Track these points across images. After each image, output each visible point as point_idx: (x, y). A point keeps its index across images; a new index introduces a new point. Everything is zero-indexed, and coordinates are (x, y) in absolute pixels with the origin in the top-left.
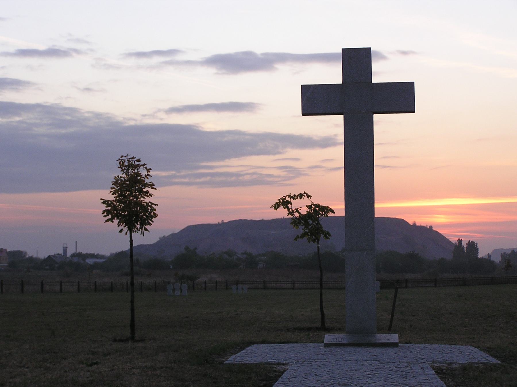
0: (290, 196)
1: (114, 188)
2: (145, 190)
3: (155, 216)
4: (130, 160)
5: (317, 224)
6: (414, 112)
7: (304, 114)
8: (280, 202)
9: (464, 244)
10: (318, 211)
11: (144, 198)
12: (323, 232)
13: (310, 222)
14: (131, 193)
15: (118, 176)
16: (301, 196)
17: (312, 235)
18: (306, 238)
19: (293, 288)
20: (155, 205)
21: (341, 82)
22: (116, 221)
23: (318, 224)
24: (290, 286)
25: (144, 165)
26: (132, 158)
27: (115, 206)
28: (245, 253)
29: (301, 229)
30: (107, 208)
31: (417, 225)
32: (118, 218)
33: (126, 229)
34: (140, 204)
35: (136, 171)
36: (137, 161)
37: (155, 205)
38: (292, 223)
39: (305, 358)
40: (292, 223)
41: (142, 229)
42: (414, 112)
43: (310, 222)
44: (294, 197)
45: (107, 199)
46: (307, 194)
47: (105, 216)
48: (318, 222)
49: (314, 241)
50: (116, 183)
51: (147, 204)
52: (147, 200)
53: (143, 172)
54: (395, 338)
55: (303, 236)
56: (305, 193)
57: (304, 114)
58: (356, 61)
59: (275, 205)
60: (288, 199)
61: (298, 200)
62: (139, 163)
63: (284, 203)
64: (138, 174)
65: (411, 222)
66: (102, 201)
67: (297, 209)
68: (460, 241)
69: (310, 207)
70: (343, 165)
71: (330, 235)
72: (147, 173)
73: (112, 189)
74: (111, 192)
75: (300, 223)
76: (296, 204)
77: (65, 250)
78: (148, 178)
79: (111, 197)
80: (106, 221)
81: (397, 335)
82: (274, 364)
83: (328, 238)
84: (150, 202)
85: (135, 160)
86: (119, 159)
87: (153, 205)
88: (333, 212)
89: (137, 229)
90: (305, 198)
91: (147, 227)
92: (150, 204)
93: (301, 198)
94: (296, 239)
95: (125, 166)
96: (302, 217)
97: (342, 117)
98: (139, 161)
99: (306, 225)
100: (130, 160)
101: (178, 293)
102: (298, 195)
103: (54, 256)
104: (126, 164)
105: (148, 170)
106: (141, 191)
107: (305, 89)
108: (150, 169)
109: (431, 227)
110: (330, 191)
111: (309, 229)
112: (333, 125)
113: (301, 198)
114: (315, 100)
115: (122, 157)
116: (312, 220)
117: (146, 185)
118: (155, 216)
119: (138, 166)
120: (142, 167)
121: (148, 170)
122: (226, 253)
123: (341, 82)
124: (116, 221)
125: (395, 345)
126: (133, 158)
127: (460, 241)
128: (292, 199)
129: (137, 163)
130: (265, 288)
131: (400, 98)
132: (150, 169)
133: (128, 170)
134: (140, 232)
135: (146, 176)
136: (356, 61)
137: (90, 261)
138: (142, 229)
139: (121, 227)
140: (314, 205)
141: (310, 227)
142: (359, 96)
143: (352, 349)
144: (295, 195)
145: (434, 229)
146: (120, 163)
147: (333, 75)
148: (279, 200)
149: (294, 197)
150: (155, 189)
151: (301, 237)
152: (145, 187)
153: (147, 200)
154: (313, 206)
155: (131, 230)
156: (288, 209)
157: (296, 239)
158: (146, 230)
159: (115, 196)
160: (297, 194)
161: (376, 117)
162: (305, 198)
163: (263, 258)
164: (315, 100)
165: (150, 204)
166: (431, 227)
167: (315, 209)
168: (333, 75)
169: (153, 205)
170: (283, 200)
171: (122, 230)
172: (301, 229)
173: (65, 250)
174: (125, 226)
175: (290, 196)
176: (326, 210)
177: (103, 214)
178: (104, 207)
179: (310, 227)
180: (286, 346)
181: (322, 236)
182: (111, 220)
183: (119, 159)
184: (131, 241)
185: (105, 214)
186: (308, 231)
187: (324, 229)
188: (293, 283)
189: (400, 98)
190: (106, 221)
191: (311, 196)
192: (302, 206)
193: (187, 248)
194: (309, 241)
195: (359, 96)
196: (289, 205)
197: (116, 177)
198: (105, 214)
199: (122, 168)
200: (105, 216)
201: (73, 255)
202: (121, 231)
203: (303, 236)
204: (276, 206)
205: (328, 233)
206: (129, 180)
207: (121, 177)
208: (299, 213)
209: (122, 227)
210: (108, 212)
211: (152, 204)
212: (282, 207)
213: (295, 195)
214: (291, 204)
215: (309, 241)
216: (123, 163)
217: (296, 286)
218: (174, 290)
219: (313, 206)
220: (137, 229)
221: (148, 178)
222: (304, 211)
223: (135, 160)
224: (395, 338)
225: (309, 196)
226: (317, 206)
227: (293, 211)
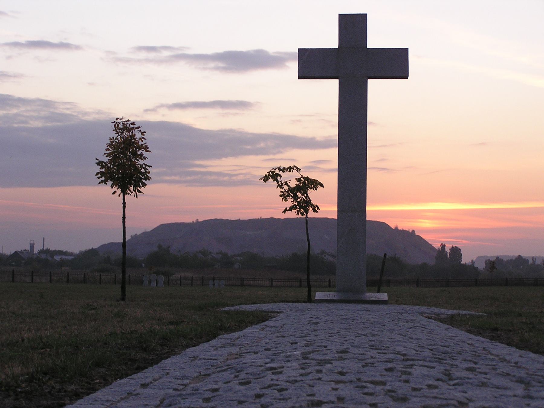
0: (279, 169)
1: (109, 150)
2: (139, 153)
3: (148, 178)
4: (125, 123)
5: (306, 197)
6: (407, 77)
7: (300, 78)
8: (269, 175)
9: (448, 249)
11: (138, 160)
12: (312, 205)
13: (299, 195)
14: (125, 156)
15: (113, 138)
16: (290, 169)
18: (294, 211)
19: (271, 286)
20: (149, 166)
21: (337, 47)
22: (110, 183)
24: (268, 283)
26: (126, 121)
27: (108, 167)
28: (221, 253)
29: (290, 202)
30: (101, 170)
31: (399, 229)
32: (111, 180)
33: (119, 191)
34: (134, 165)
37: (149, 166)
38: (280, 196)
39: (298, 307)
40: (280, 196)
41: (135, 191)
42: (407, 77)
43: (299, 195)
44: (283, 170)
45: (101, 160)
47: (99, 178)
48: (307, 195)
49: (303, 214)
50: (110, 145)
51: (141, 166)
52: (141, 162)
53: (138, 135)
54: (384, 296)
55: (291, 209)
56: (294, 166)
57: (300, 78)
58: (353, 26)
59: (264, 177)
60: (277, 171)
61: (288, 173)
63: (273, 176)
64: (133, 136)
65: (393, 226)
66: (98, 161)
68: (443, 246)
69: (299, 180)
70: (334, 132)
71: (318, 209)
72: (141, 136)
73: (106, 150)
74: (105, 154)
75: (289, 196)
76: (285, 176)
77: (32, 246)
78: (142, 141)
79: (106, 159)
80: (100, 183)
81: (386, 294)
82: (269, 312)
83: (316, 211)
84: (144, 164)
85: (129, 123)
86: (115, 122)
87: (147, 167)
88: (322, 185)
89: (130, 191)
91: (142, 189)
92: (144, 166)
93: (290, 171)
94: (284, 212)
95: (120, 129)
96: (291, 190)
97: (337, 81)
98: (133, 124)
99: (295, 197)
100: (125, 123)
101: (154, 284)
103: (21, 252)
104: (121, 126)
105: (143, 133)
106: (135, 154)
108: (145, 132)
109: (413, 231)
111: (298, 202)
112: (328, 91)
114: (312, 64)
115: (117, 119)
116: (301, 193)
117: (140, 147)
118: (148, 178)
119: (133, 128)
120: (137, 130)
121: (143, 133)
122: (200, 252)
123: (337, 47)
124: (110, 183)
125: (384, 302)
126: (128, 121)
127: (443, 246)
128: (281, 172)
129: (131, 126)
130: (242, 285)
131: (394, 64)
132: (145, 132)
133: (123, 132)
134: (133, 194)
135: (140, 139)
136: (353, 26)
137: (57, 258)
138: (135, 191)
139: (115, 189)
141: (299, 200)
142: (354, 62)
143: (343, 305)
144: (284, 168)
145: (417, 234)
147: (329, 39)
148: (269, 172)
150: (150, 151)
151: (289, 210)
152: (140, 149)
153: (141, 162)
154: (302, 179)
155: (124, 192)
156: (278, 182)
157: (284, 212)
158: (139, 192)
159: (108, 158)
160: (287, 167)
164: (312, 64)
165: (144, 166)
166: (413, 231)
167: (304, 182)
168: (329, 39)
169: (147, 167)
170: (273, 172)
171: (115, 191)
172: (290, 202)
173: (32, 246)
174: (119, 188)
176: (315, 184)
177: (97, 175)
178: (98, 169)
179: (299, 200)
181: (311, 209)
182: (105, 182)
184: (124, 203)
185: (99, 175)
186: (296, 204)
187: (312, 202)
188: (271, 280)
189: (394, 64)
190: (100, 183)
191: (300, 170)
193: (160, 247)
194: (298, 214)
195: (354, 62)
197: (111, 139)
198: (99, 175)
199: (116, 131)
200: (99, 178)
201: (42, 252)
202: (114, 193)
203: (291, 209)
204: (265, 179)
205: (317, 206)
206: (124, 142)
207: (116, 139)
208: (289, 186)
210: (102, 174)
211: (146, 165)
214: (281, 176)
215: (298, 214)
216: (118, 125)
217: (274, 283)
218: (150, 282)
219: (302, 179)
220: (130, 191)
221: (142, 141)
222: (293, 184)
223: (129, 123)
224: (384, 296)
225: (298, 170)
226: (307, 179)
227: (282, 184)
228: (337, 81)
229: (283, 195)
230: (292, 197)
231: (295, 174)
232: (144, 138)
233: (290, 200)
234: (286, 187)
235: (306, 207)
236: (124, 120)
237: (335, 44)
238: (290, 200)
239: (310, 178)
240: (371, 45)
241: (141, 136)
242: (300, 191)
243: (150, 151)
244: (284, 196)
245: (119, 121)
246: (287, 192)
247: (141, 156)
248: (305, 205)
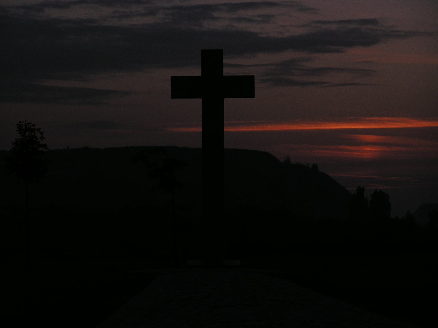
25: (39, 129)
26: (29, 124)
35: (33, 134)
53: (38, 135)
58: (212, 59)
62: (35, 127)
72: (41, 136)
78: (42, 140)
85: (30, 125)
98: (34, 125)
105: (42, 133)
108: (43, 132)
114: (181, 88)
115: (20, 122)
121: (42, 133)
123: (200, 75)
126: (30, 123)
129: (32, 127)
131: (244, 87)
135: (41, 138)
146: (18, 127)
161: (226, 100)
164: (181, 88)
183: (18, 124)
189: (244, 87)
195: (214, 84)
221: (42, 140)
232: (43, 138)
241: (41, 136)
243: (48, 149)
245: (22, 123)
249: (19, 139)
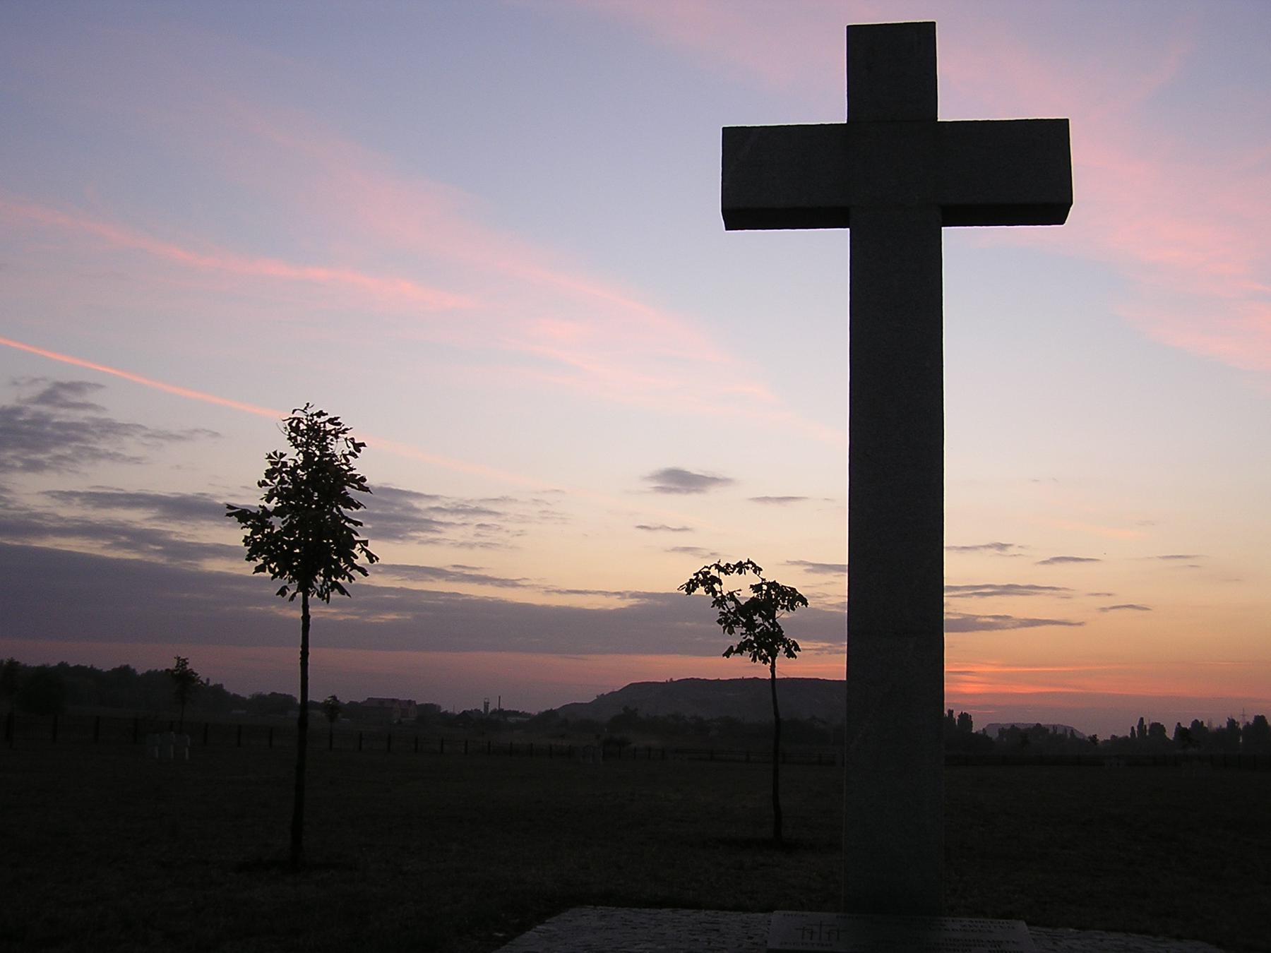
10: (775, 597)
12: (785, 641)
15: (275, 453)
16: (741, 567)
17: (760, 648)
18: (746, 652)
23: (775, 625)
36: (331, 421)
37: (357, 523)
38: (720, 622)
40: (720, 622)
43: (758, 619)
44: (726, 570)
46: (754, 565)
49: (766, 661)
53: (339, 447)
55: (741, 649)
56: (749, 562)
58: (891, 61)
59: (688, 584)
60: (714, 572)
63: (706, 580)
67: (731, 594)
69: (756, 588)
71: (797, 649)
75: (737, 622)
85: (323, 419)
88: (804, 602)
90: (750, 572)
93: (740, 572)
94: (727, 654)
97: (842, 236)
99: (750, 626)
102: (735, 566)
107: (733, 138)
108: (363, 445)
110: (803, 535)
113: (740, 572)
114: (767, 180)
126: (320, 414)
129: (329, 427)
132: (363, 445)
136: (891, 61)
140: (768, 584)
144: (728, 565)
146: (290, 424)
148: (696, 574)
149: (726, 570)
154: (765, 587)
155: (305, 587)
158: (343, 591)
160: (733, 562)
162: (750, 572)
163: (377, 512)
167: (768, 591)
172: (737, 637)
175: (717, 566)
176: (793, 598)
180: (666, 913)
191: (760, 569)
192: (740, 586)
194: (754, 660)
196: (716, 586)
197: (270, 457)
202: (282, 592)
204: (691, 586)
208: (737, 602)
209: (286, 582)
212: (701, 590)
213: (728, 565)
215: (754, 660)
219: (765, 587)
222: (747, 594)
223: (327, 418)
225: (757, 569)
226: (773, 585)
228: (842, 236)
229: (726, 621)
230: (744, 624)
231: (751, 578)
233: (739, 630)
234: (731, 604)
235: (772, 644)
236: (309, 411)
237: (835, 111)
238: (739, 630)
239: (781, 584)
240: (947, 112)
242: (761, 617)
244: (728, 623)
245: (298, 414)
246: (734, 614)
247: (350, 503)
248: (769, 642)
249: (275, 453)
